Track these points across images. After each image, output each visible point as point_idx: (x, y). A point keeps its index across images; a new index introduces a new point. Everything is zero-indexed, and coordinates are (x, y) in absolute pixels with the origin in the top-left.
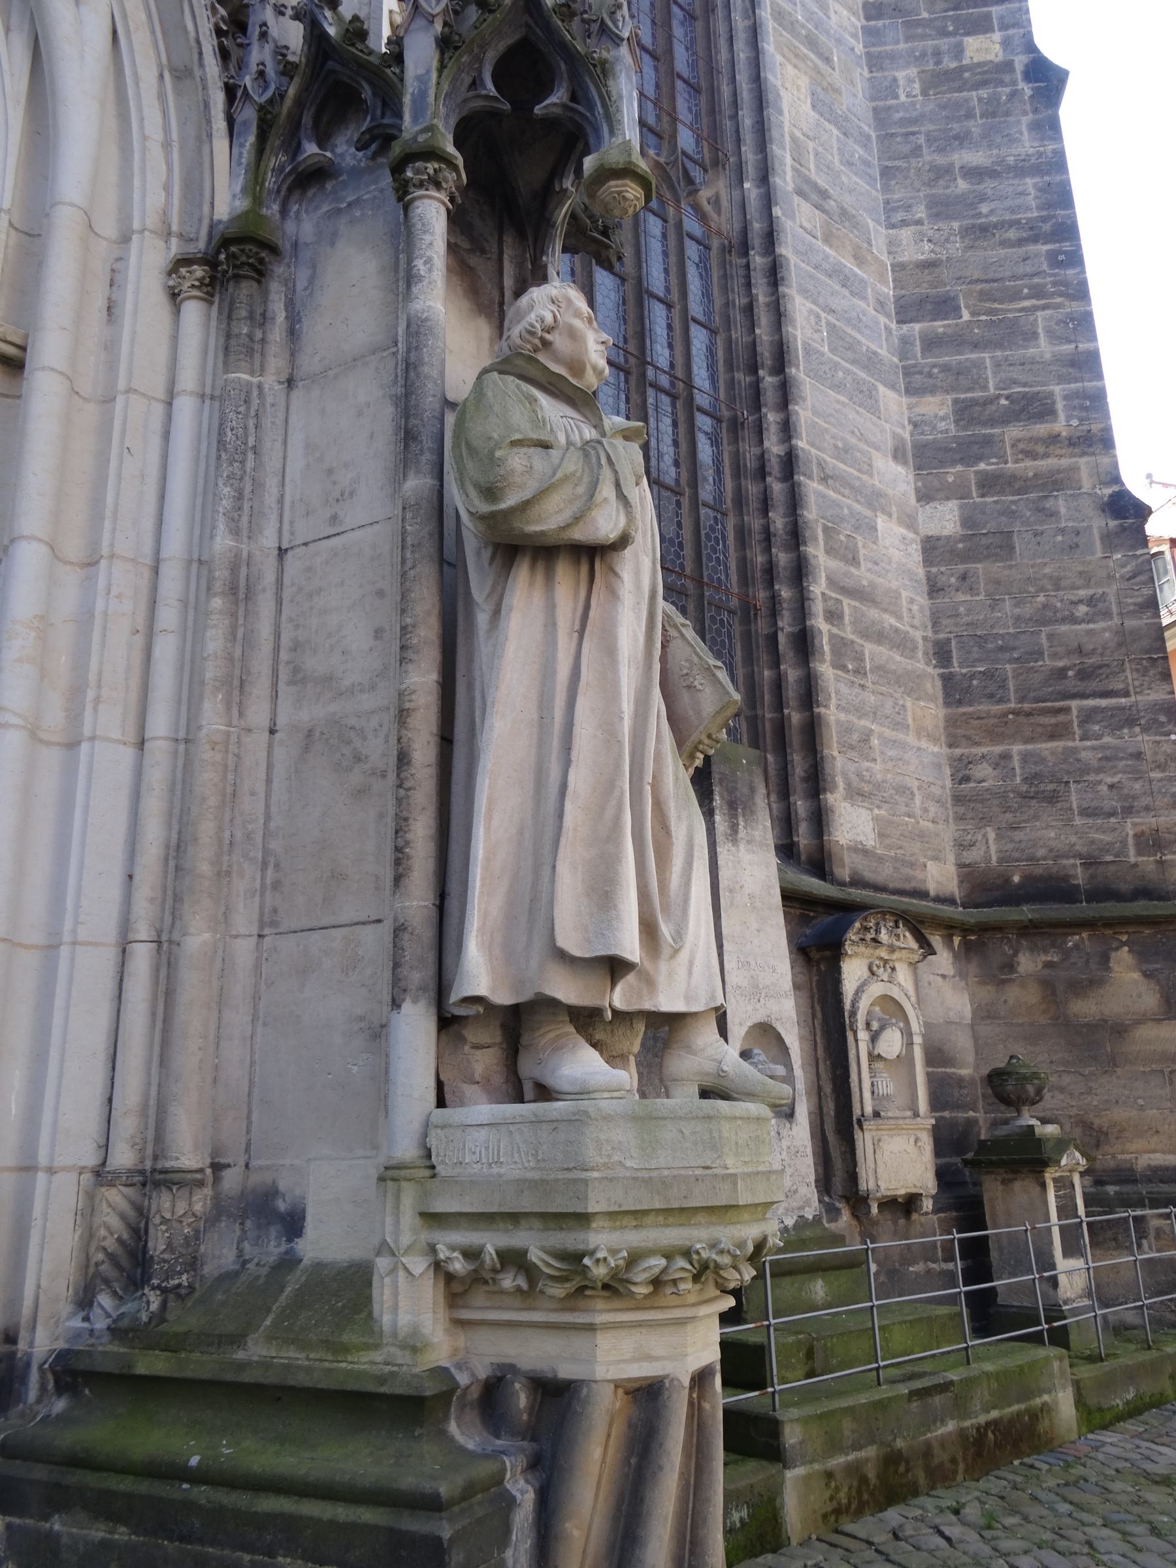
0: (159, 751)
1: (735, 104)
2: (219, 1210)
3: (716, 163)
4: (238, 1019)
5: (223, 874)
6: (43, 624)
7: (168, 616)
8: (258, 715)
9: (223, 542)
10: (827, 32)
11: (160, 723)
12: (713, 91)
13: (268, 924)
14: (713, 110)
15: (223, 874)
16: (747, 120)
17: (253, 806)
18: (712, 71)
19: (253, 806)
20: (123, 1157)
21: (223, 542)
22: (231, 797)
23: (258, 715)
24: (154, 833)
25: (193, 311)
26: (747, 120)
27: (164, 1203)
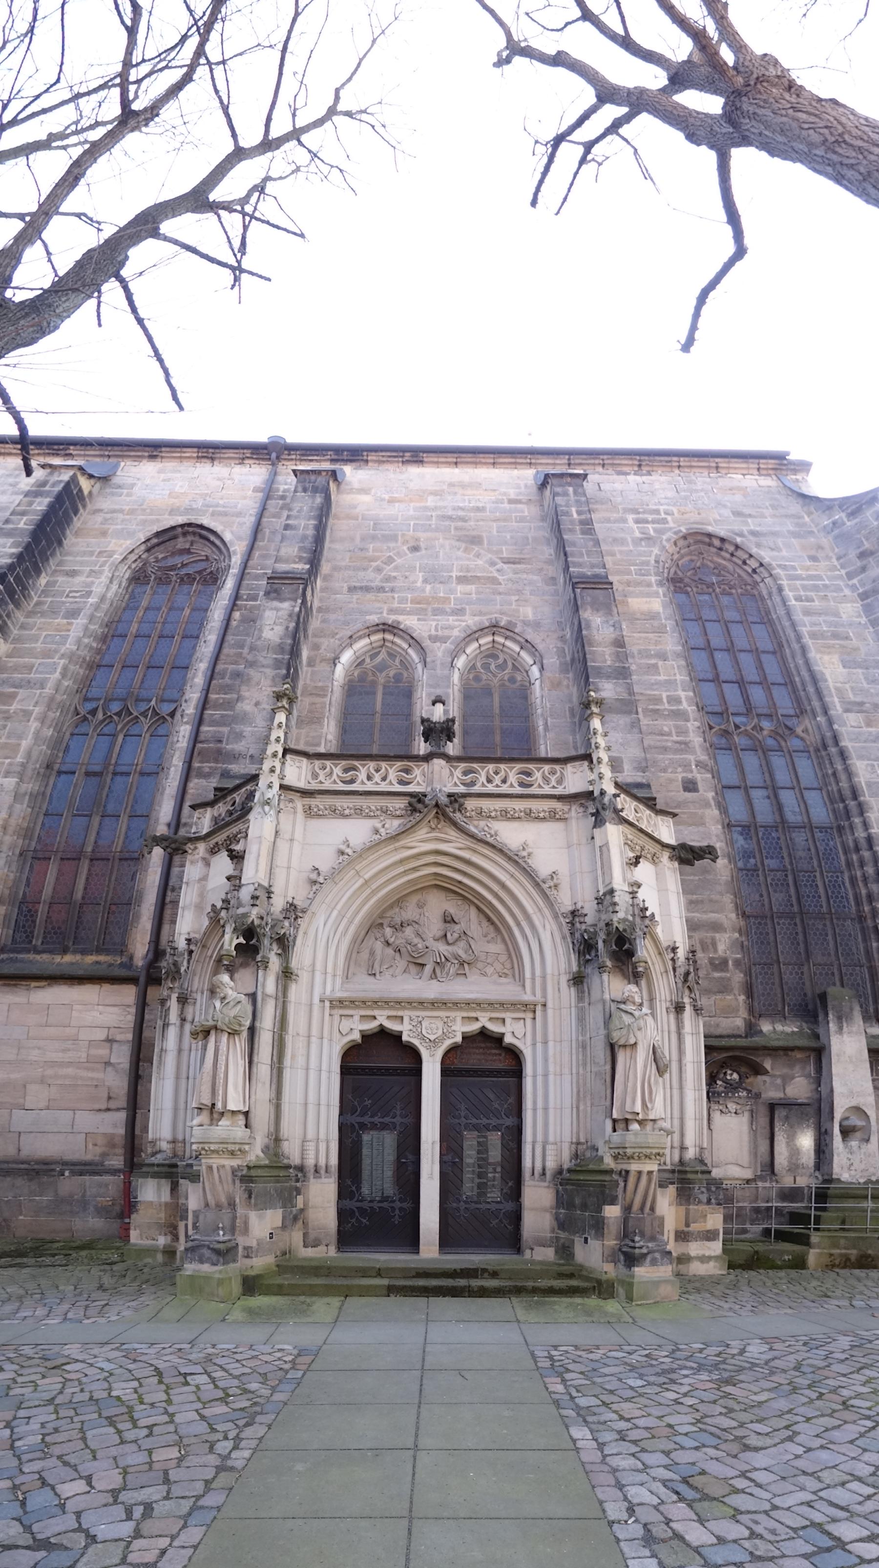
0: (574, 1075)
1: (803, 684)
2: (587, 1148)
3: (802, 713)
4: (589, 1120)
5: (585, 1097)
6: (555, 1054)
7: (574, 1051)
8: (588, 1069)
9: (580, 1038)
10: (843, 625)
11: (574, 1071)
12: (792, 683)
13: (592, 1105)
14: (795, 690)
15: (585, 1097)
16: (811, 689)
17: (588, 1085)
18: (789, 674)
19: (588, 1085)
20: (574, 1140)
21: (580, 1038)
22: (585, 1084)
23: (588, 1069)
24: (575, 1090)
25: (572, 989)
26: (811, 689)
27: (580, 1147)
